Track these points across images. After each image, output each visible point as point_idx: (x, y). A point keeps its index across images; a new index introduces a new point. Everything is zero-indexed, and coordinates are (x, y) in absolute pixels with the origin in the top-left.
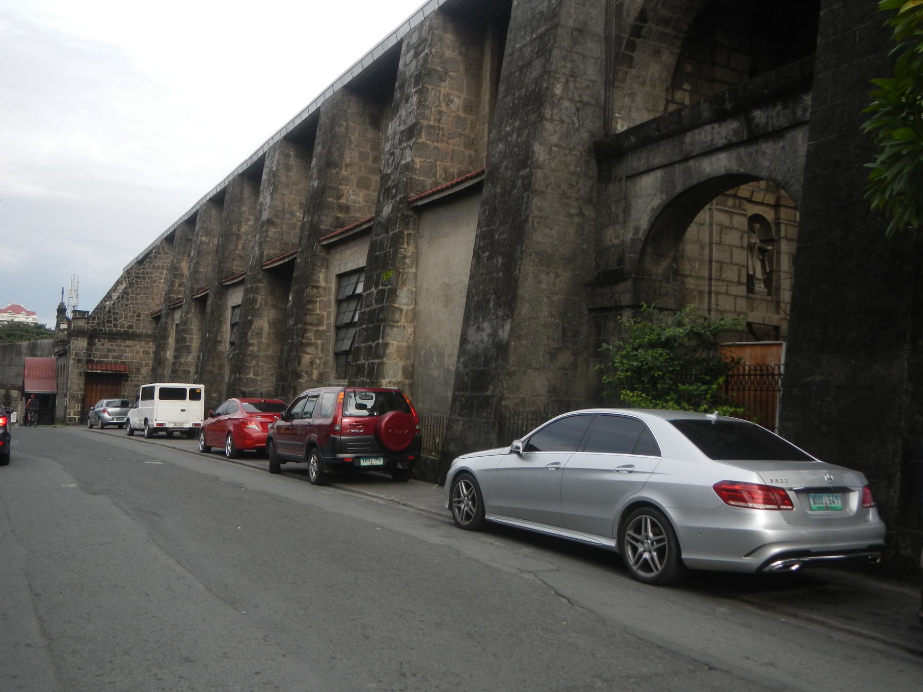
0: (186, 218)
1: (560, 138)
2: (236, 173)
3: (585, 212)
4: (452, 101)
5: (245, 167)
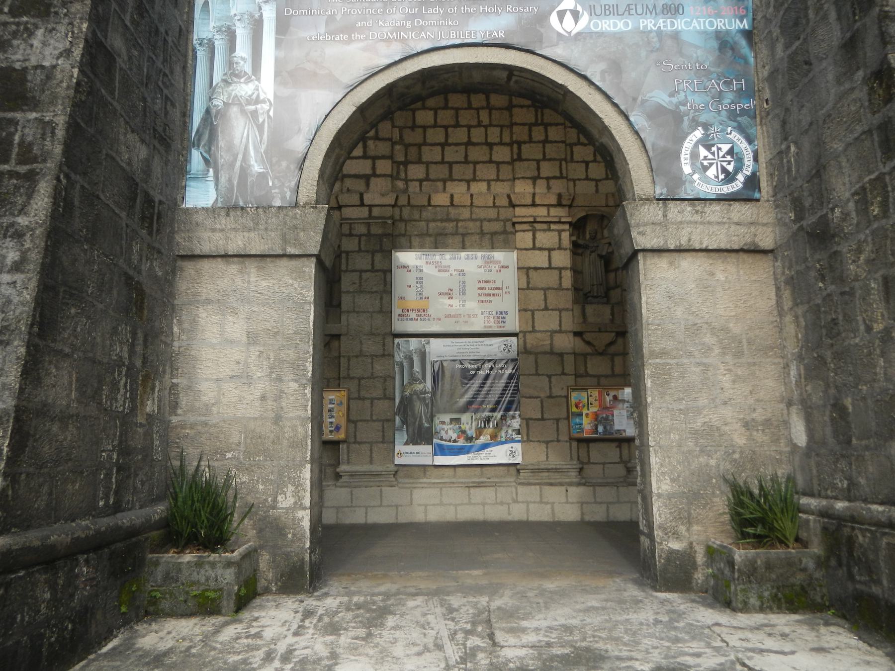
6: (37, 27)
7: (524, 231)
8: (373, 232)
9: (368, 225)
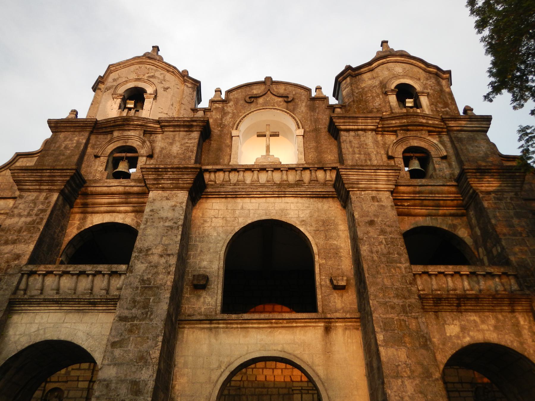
6: (144, 367)
7: (297, 394)
8: (231, 393)
9: (229, 390)
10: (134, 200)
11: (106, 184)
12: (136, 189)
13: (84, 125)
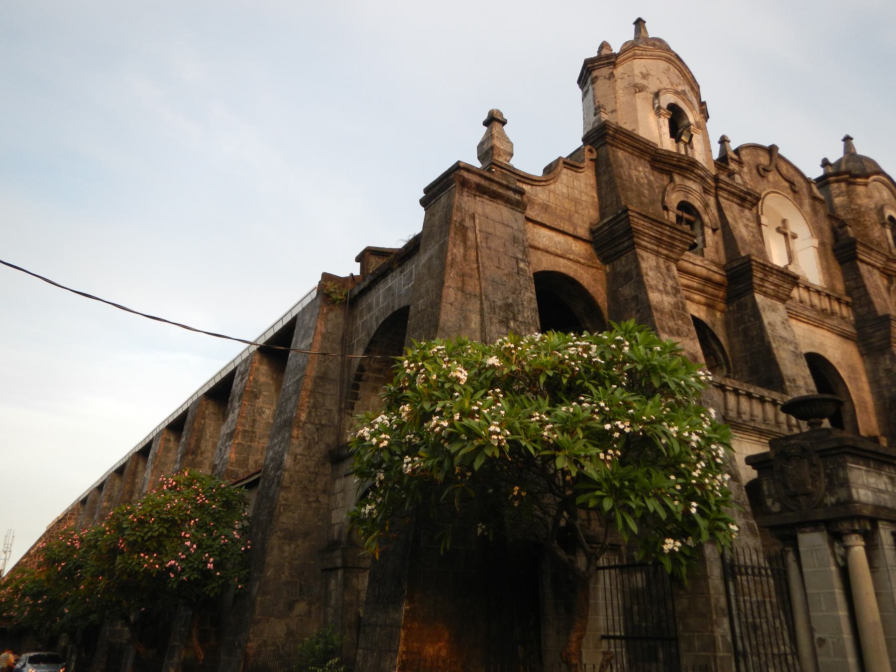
0: (97, 485)
1: (304, 449)
2: (134, 451)
3: (320, 499)
4: (264, 412)
5: (140, 447)
10: (710, 290)
11: (691, 260)
12: (717, 277)
13: (645, 149)
